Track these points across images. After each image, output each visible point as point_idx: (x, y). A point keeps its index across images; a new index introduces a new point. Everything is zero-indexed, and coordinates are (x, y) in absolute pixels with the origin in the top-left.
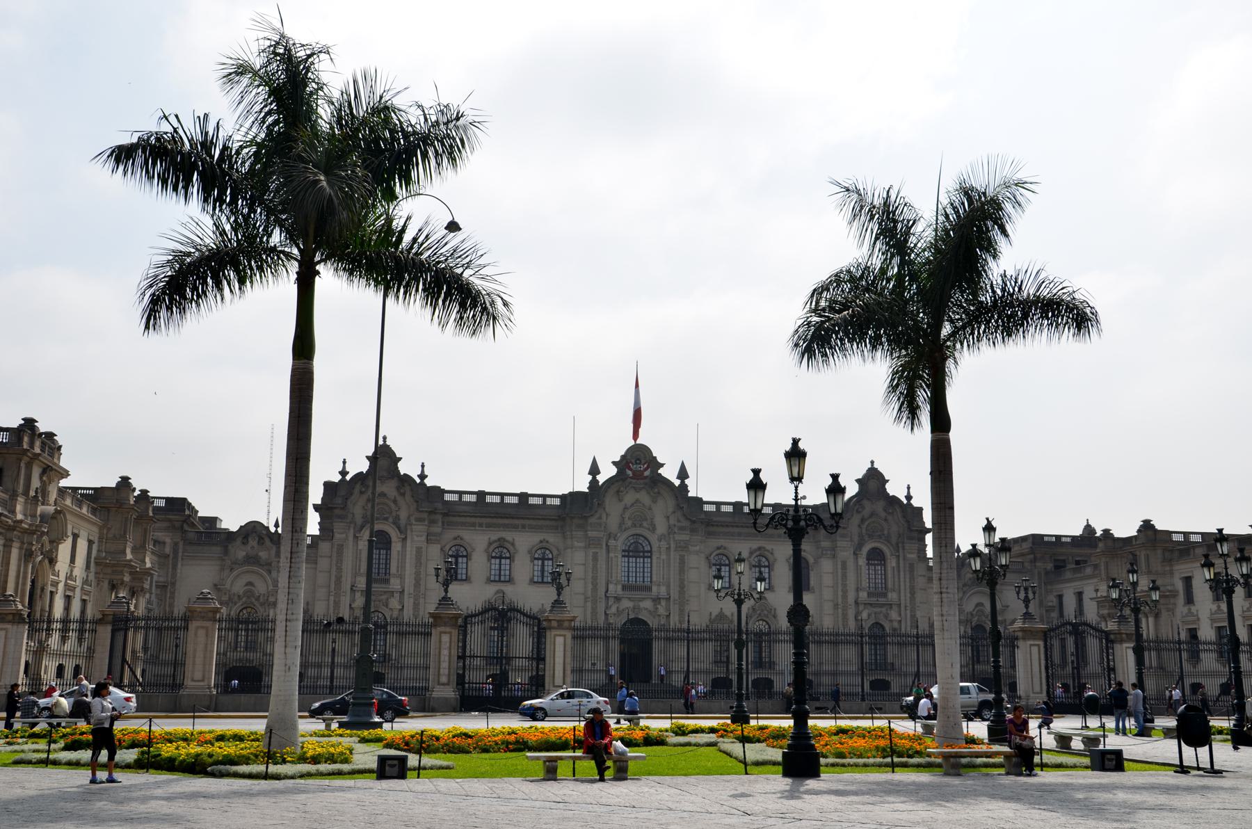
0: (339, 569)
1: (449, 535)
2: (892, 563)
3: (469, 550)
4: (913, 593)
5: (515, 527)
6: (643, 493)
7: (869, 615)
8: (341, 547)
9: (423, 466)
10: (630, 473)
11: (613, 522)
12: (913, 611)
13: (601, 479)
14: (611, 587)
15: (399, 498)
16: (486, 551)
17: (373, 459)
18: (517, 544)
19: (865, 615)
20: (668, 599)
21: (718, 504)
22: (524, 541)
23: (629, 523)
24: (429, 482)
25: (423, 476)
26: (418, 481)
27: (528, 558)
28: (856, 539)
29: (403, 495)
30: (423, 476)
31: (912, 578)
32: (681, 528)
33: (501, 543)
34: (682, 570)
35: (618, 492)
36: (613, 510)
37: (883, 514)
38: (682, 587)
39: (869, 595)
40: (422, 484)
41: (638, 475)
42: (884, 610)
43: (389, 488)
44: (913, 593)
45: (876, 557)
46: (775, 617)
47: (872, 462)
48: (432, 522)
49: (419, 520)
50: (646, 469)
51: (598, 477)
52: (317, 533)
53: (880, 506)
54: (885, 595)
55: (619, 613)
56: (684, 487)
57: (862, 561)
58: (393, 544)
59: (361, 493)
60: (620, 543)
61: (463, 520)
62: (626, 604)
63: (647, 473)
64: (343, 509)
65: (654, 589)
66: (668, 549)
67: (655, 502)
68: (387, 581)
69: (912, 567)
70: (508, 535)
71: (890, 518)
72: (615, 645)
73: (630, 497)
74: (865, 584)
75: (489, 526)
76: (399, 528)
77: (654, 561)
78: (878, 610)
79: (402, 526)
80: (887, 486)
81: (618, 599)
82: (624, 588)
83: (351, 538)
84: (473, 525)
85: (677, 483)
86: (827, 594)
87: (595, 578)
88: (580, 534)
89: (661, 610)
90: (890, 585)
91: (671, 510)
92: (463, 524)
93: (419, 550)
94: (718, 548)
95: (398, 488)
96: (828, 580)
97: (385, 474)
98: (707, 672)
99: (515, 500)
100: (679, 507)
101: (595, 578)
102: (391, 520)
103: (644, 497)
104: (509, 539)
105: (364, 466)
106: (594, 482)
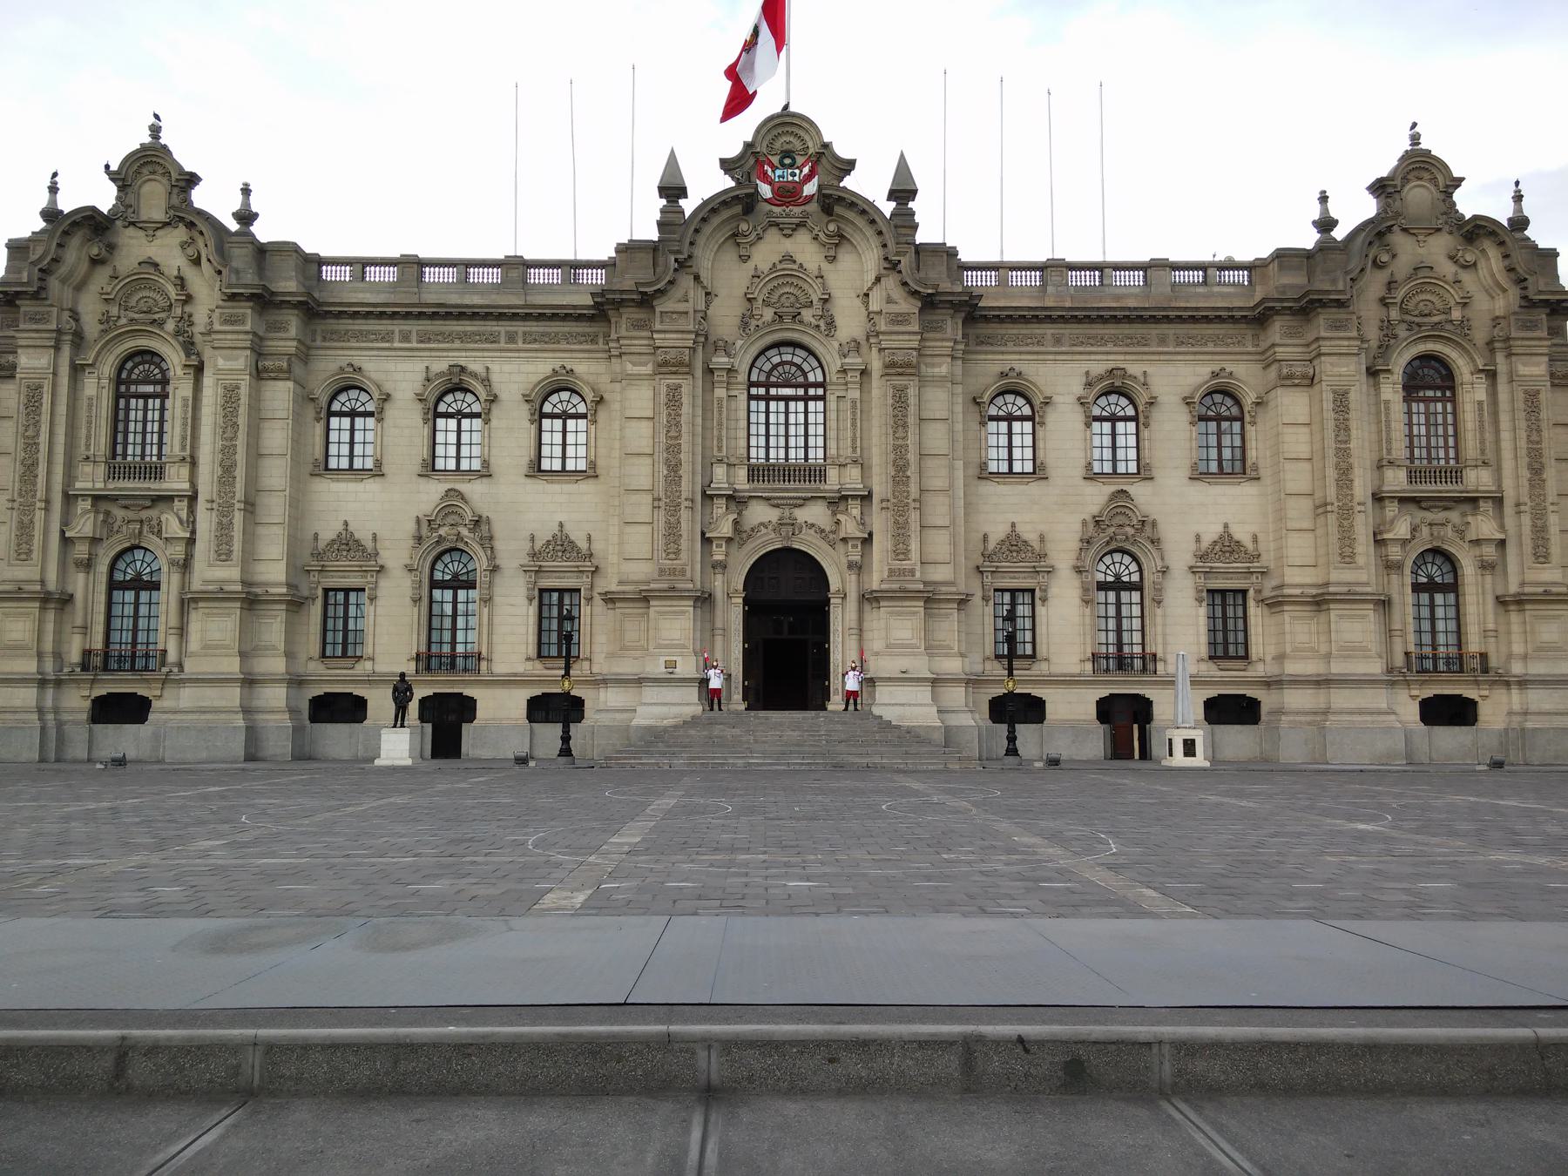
0: (31, 445)
1: (329, 364)
2: (1472, 392)
3: (376, 395)
4: (1537, 470)
7: (1414, 529)
9: (246, 191)
10: (765, 190)
11: (725, 316)
12: (1539, 515)
13: (689, 205)
14: (720, 472)
15: (190, 273)
18: (494, 378)
19: (1402, 529)
20: (866, 498)
22: (514, 372)
23: (768, 314)
24: (263, 232)
26: (233, 226)
27: (523, 412)
28: (1373, 334)
29: (197, 262)
30: (246, 217)
31: (1534, 428)
32: (899, 319)
33: (456, 383)
34: (899, 422)
35: (735, 235)
36: (729, 280)
38: (900, 467)
39: (1413, 476)
40: (245, 235)
41: (788, 194)
42: (1454, 516)
43: (168, 250)
44: (1537, 470)
45: (1430, 379)
46: (1155, 542)
50: (809, 178)
51: (682, 202)
53: (1437, 250)
54: (1456, 475)
55: (740, 535)
56: (905, 220)
57: (1392, 391)
59: (96, 262)
62: (759, 513)
63: (810, 189)
64: (38, 295)
65: (832, 473)
66: (864, 373)
67: (832, 259)
68: (157, 472)
69: (1532, 398)
72: (732, 615)
73: (768, 251)
74: (1399, 450)
76: (189, 347)
77: (832, 405)
78: (1439, 516)
79: (198, 339)
80: (1457, 196)
81: (736, 500)
82: (754, 473)
83: (64, 370)
84: (387, 337)
85: (887, 208)
86: (1298, 478)
87: (673, 449)
88: (639, 343)
89: (850, 527)
90: (1471, 448)
91: (871, 277)
92: (361, 336)
93: (230, 394)
94: (1003, 375)
95: (184, 246)
96: (1298, 442)
97: (159, 215)
98: (973, 682)
99: (492, 276)
100: (893, 266)
101: (673, 449)
102: (170, 326)
103: (804, 249)
104: (475, 366)
105: (105, 197)
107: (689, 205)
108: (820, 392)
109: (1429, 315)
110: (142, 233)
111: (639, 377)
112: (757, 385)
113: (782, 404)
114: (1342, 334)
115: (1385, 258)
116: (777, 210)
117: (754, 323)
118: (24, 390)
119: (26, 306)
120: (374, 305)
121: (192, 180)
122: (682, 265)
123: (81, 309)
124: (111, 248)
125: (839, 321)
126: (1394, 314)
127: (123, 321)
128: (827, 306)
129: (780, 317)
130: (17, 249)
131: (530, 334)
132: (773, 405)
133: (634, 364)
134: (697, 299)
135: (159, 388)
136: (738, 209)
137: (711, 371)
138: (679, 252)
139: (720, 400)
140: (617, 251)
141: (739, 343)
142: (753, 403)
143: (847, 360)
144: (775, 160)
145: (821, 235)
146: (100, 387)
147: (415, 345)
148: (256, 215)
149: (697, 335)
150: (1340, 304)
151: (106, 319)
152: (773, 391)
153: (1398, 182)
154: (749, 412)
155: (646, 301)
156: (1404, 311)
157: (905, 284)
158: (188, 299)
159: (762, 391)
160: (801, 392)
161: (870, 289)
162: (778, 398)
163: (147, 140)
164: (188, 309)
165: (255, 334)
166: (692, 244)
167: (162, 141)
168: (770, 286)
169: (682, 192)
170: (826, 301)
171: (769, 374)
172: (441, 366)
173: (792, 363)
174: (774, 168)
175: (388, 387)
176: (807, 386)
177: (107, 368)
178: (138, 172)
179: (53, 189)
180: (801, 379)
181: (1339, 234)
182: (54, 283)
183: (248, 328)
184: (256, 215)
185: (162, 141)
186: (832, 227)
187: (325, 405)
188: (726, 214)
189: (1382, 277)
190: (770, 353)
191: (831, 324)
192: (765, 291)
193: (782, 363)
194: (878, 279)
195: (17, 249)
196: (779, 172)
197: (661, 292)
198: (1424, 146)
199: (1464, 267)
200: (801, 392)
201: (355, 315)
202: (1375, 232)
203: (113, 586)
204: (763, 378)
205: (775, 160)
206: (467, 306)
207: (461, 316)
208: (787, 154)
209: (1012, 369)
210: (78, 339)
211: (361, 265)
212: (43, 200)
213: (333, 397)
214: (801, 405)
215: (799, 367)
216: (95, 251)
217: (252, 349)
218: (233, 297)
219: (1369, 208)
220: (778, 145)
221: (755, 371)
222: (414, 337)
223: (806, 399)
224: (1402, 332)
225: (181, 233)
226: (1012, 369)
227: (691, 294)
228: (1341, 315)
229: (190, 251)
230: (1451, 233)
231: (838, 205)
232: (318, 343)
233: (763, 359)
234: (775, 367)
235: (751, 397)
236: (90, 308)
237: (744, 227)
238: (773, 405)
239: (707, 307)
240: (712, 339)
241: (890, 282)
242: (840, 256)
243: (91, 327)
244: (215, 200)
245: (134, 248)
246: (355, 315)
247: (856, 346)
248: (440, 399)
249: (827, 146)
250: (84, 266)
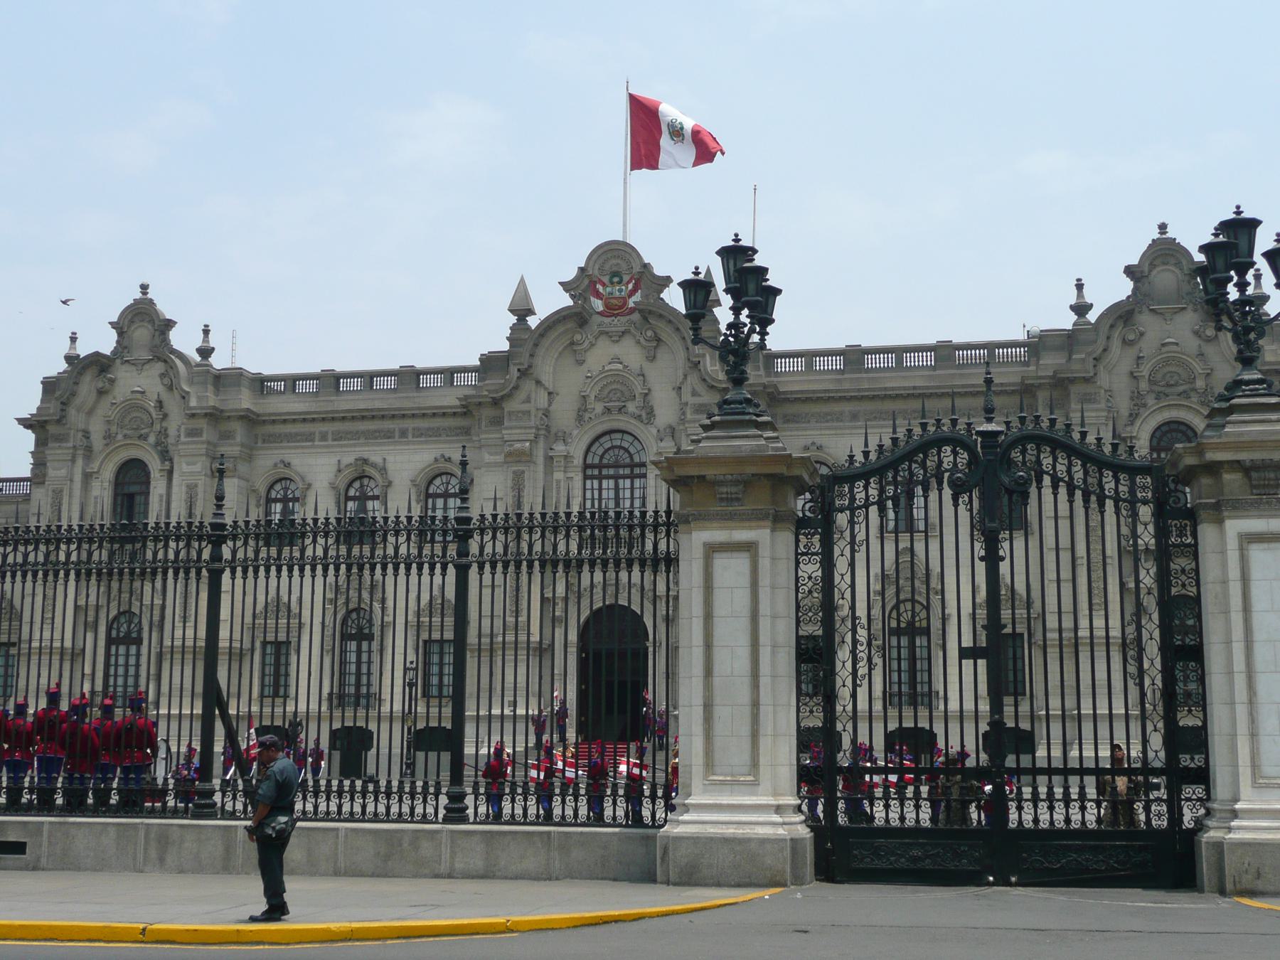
1: (266, 461)
5: (388, 435)
6: (628, 342)
8: (58, 494)
10: (598, 305)
11: (564, 413)
13: (533, 322)
15: (165, 396)
16: (333, 487)
17: (120, 327)
18: (390, 467)
21: (809, 356)
23: (599, 408)
24: (219, 361)
25: (205, 352)
28: (1124, 406)
30: (205, 352)
35: (572, 343)
36: (565, 382)
37: (1192, 344)
47: (1163, 227)
48: (227, 436)
49: (193, 433)
52: (26, 472)
58: (153, 483)
59: (101, 393)
60: (577, 451)
61: (289, 428)
64: (59, 422)
67: (652, 358)
70: (376, 454)
71: (1209, 350)
72: (567, 664)
73: (600, 356)
75: (338, 437)
76: (165, 455)
79: (170, 448)
83: (78, 477)
84: (309, 437)
91: (680, 373)
92: (291, 437)
95: (162, 376)
102: (152, 439)
103: (631, 353)
104: (376, 458)
105: (106, 342)
106: (519, 333)
107: (533, 322)
108: (643, 470)
109: (1176, 384)
110: (134, 368)
111: (496, 464)
112: (592, 466)
113: (612, 482)
114: (1095, 406)
115: (1131, 337)
116: (607, 320)
117: (587, 416)
118: (50, 493)
119: (52, 429)
120: (300, 413)
121: (170, 324)
122: (524, 373)
123: (91, 428)
124: (112, 381)
125: (656, 412)
126: (1144, 385)
127: (120, 437)
128: (649, 397)
129: (608, 410)
130: (49, 386)
131: (419, 429)
132: (605, 483)
133: (491, 454)
134: (542, 399)
135: (144, 487)
136: (571, 325)
137: (552, 458)
138: (521, 364)
139: (558, 482)
140: (480, 360)
141: (575, 432)
142: (588, 483)
143: (662, 444)
144: (606, 279)
145: (642, 340)
146: (103, 489)
147: (330, 443)
148: (213, 349)
149: (538, 429)
150: (1087, 380)
151: (109, 437)
152: (605, 472)
153: (1146, 269)
154: (585, 489)
155: (496, 403)
156: (1151, 382)
157: (704, 380)
158: (165, 416)
159: (596, 472)
160: (627, 471)
161: (682, 383)
162: (608, 477)
163: (138, 295)
164: (164, 424)
165: (209, 443)
166: (532, 355)
167: (149, 296)
168: (601, 385)
169: (531, 312)
170: (646, 395)
171: (602, 457)
172: (349, 459)
173: (621, 447)
174: (604, 285)
175: (309, 479)
176: (632, 466)
177: (109, 472)
178: (132, 322)
179: (73, 339)
180: (628, 460)
181: (1092, 316)
182: (72, 412)
183: (204, 438)
184: (213, 349)
185: (149, 296)
186: (649, 333)
187: (263, 494)
188: (561, 328)
189: (1132, 352)
190: (602, 440)
191: (651, 413)
192: (597, 388)
193: (613, 447)
194: (685, 376)
195: (49, 386)
196: (609, 289)
197: (509, 396)
198: (1171, 233)
199: (1209, 340)
200: (627, 471)
201: (285, 421)
202: (1121, 314)
203: (110, 641)
204: (597, 461)
205: (606, 279)
206: (367, 410)
207: (363, 418)
208: (615, 274)
209: (813, 443)
210: (89, 450)
211: (292, 381)
212: (65, 348)
213: (271, 487)
214: (628, 482)
215: (627, 450)
216: (100, 385)
217: (207, 455)
218: (193, 415)
219: (1124, 288)
220: (607, 267)
221: (590, 455)
222: (330, 436)
223: (632, 477)
224: (1150, 401)
225: (159, 367)
226: (813, 443)
227: (533, 395)
228: (1089, 389)
229: (166, 381)
230: (1195, 311)
231: (655, 312)
232: (259, 444)
233: (597, 444)
234: (606, 451)
235: (586, 478)
236: (97, 429)
237: (578, 337)
238: (605, 483)
239: (550, 404)
240: (554, 430)
241: (693, 380)
242: (659, 355)
243: (97, 441)
244: (184, 340)
245: (129, 381)
246: (285, 421)
247: (672, 431)
248: (350, 485)
249: (646, 267)
250: (94, 395)
